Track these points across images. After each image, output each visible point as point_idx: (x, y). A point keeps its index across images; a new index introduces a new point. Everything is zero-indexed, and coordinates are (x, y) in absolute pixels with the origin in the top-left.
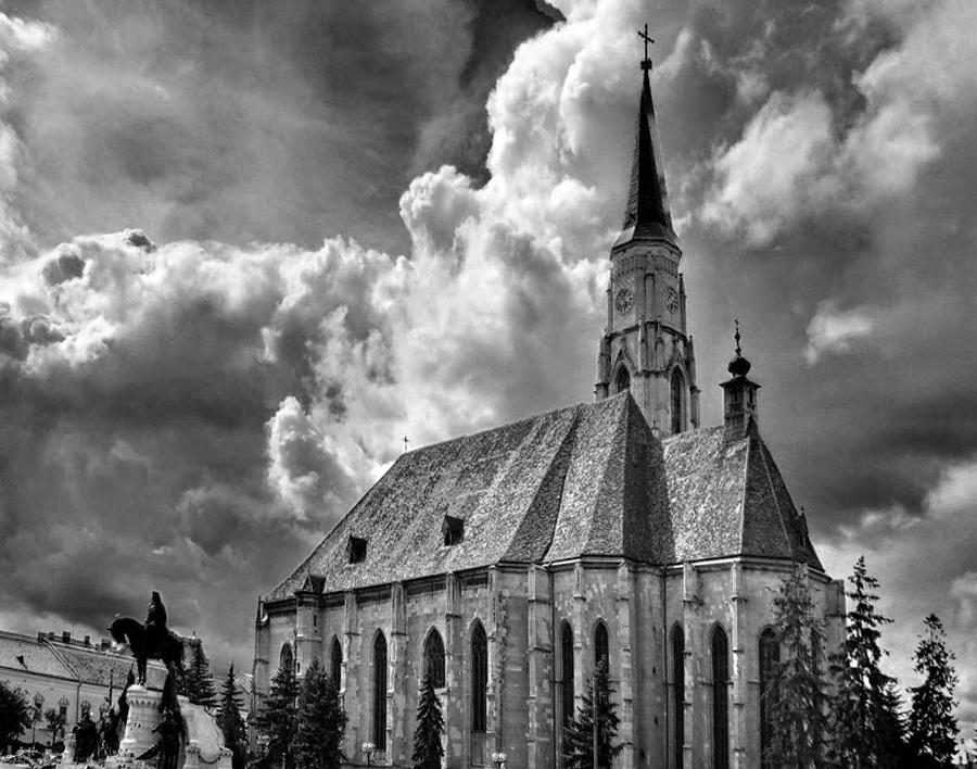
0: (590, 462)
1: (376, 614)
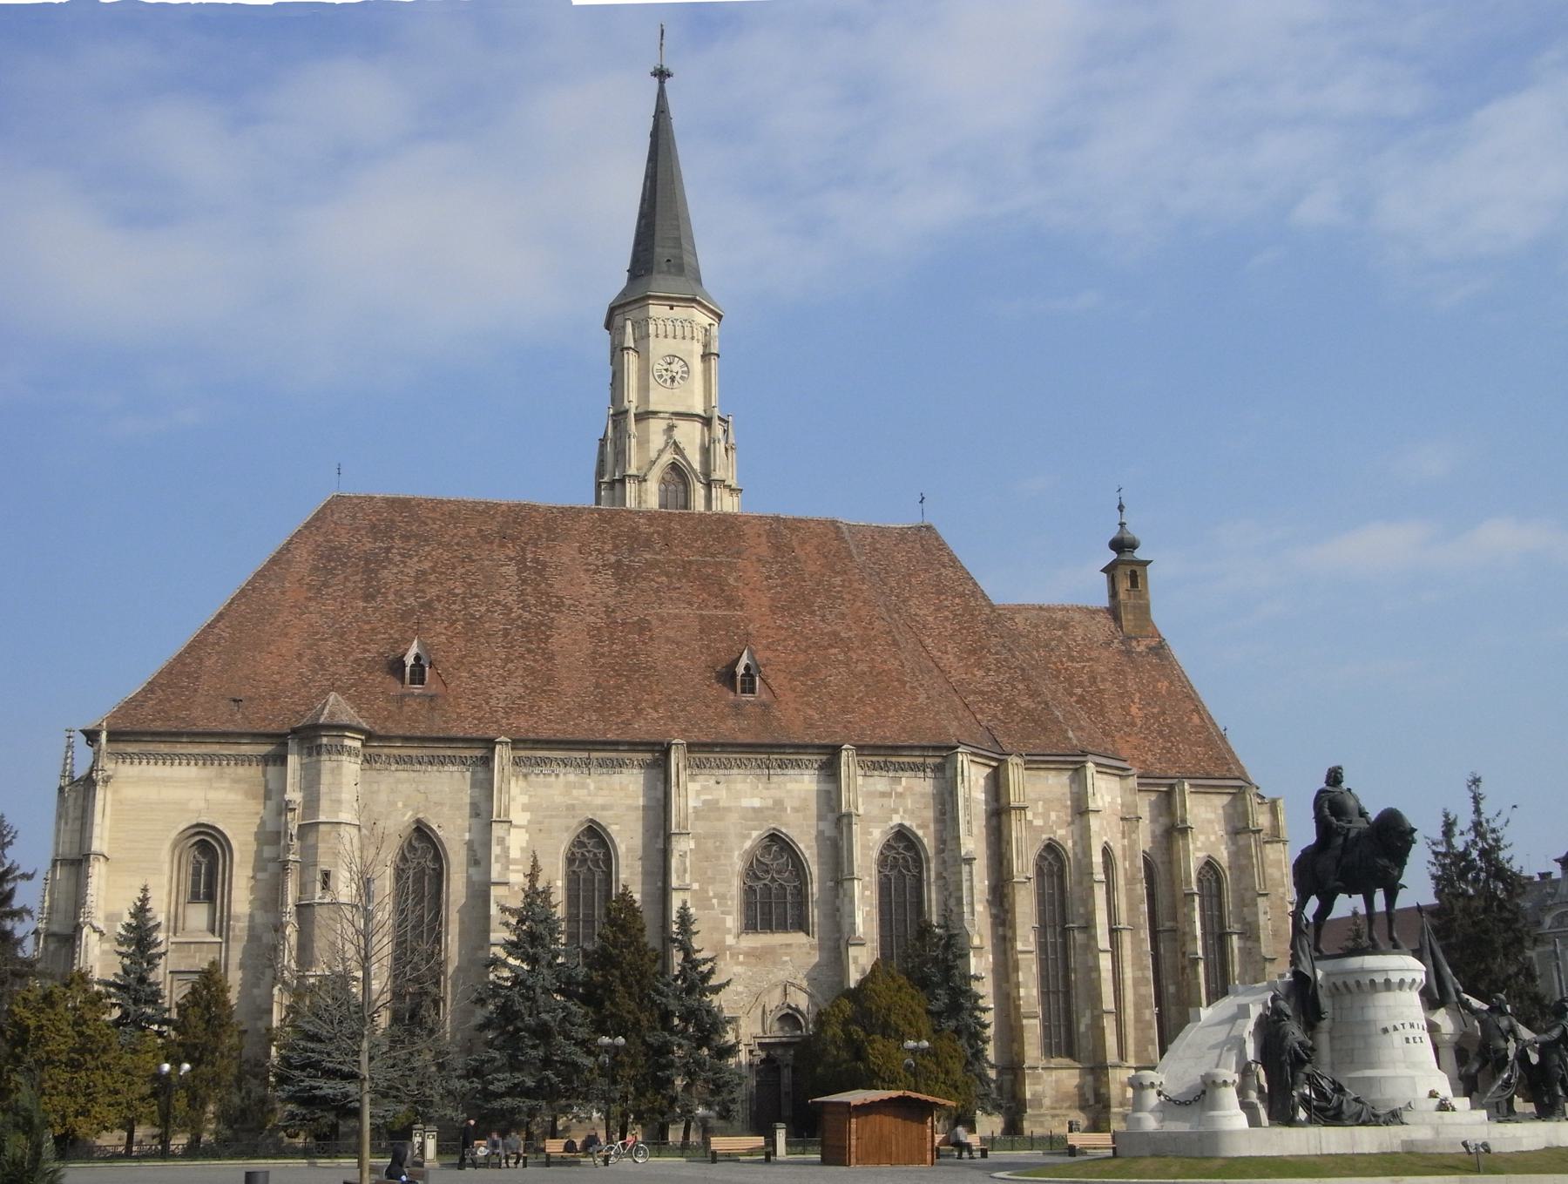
0: (947, 613)
1: (575, 792)
